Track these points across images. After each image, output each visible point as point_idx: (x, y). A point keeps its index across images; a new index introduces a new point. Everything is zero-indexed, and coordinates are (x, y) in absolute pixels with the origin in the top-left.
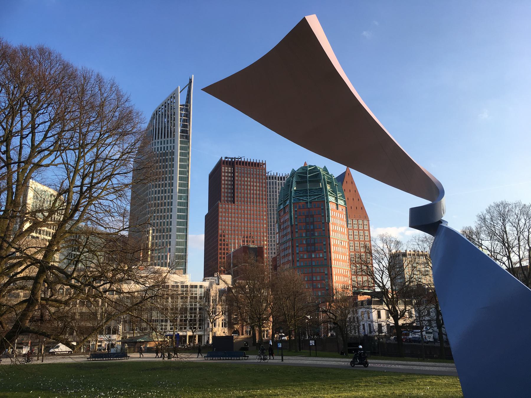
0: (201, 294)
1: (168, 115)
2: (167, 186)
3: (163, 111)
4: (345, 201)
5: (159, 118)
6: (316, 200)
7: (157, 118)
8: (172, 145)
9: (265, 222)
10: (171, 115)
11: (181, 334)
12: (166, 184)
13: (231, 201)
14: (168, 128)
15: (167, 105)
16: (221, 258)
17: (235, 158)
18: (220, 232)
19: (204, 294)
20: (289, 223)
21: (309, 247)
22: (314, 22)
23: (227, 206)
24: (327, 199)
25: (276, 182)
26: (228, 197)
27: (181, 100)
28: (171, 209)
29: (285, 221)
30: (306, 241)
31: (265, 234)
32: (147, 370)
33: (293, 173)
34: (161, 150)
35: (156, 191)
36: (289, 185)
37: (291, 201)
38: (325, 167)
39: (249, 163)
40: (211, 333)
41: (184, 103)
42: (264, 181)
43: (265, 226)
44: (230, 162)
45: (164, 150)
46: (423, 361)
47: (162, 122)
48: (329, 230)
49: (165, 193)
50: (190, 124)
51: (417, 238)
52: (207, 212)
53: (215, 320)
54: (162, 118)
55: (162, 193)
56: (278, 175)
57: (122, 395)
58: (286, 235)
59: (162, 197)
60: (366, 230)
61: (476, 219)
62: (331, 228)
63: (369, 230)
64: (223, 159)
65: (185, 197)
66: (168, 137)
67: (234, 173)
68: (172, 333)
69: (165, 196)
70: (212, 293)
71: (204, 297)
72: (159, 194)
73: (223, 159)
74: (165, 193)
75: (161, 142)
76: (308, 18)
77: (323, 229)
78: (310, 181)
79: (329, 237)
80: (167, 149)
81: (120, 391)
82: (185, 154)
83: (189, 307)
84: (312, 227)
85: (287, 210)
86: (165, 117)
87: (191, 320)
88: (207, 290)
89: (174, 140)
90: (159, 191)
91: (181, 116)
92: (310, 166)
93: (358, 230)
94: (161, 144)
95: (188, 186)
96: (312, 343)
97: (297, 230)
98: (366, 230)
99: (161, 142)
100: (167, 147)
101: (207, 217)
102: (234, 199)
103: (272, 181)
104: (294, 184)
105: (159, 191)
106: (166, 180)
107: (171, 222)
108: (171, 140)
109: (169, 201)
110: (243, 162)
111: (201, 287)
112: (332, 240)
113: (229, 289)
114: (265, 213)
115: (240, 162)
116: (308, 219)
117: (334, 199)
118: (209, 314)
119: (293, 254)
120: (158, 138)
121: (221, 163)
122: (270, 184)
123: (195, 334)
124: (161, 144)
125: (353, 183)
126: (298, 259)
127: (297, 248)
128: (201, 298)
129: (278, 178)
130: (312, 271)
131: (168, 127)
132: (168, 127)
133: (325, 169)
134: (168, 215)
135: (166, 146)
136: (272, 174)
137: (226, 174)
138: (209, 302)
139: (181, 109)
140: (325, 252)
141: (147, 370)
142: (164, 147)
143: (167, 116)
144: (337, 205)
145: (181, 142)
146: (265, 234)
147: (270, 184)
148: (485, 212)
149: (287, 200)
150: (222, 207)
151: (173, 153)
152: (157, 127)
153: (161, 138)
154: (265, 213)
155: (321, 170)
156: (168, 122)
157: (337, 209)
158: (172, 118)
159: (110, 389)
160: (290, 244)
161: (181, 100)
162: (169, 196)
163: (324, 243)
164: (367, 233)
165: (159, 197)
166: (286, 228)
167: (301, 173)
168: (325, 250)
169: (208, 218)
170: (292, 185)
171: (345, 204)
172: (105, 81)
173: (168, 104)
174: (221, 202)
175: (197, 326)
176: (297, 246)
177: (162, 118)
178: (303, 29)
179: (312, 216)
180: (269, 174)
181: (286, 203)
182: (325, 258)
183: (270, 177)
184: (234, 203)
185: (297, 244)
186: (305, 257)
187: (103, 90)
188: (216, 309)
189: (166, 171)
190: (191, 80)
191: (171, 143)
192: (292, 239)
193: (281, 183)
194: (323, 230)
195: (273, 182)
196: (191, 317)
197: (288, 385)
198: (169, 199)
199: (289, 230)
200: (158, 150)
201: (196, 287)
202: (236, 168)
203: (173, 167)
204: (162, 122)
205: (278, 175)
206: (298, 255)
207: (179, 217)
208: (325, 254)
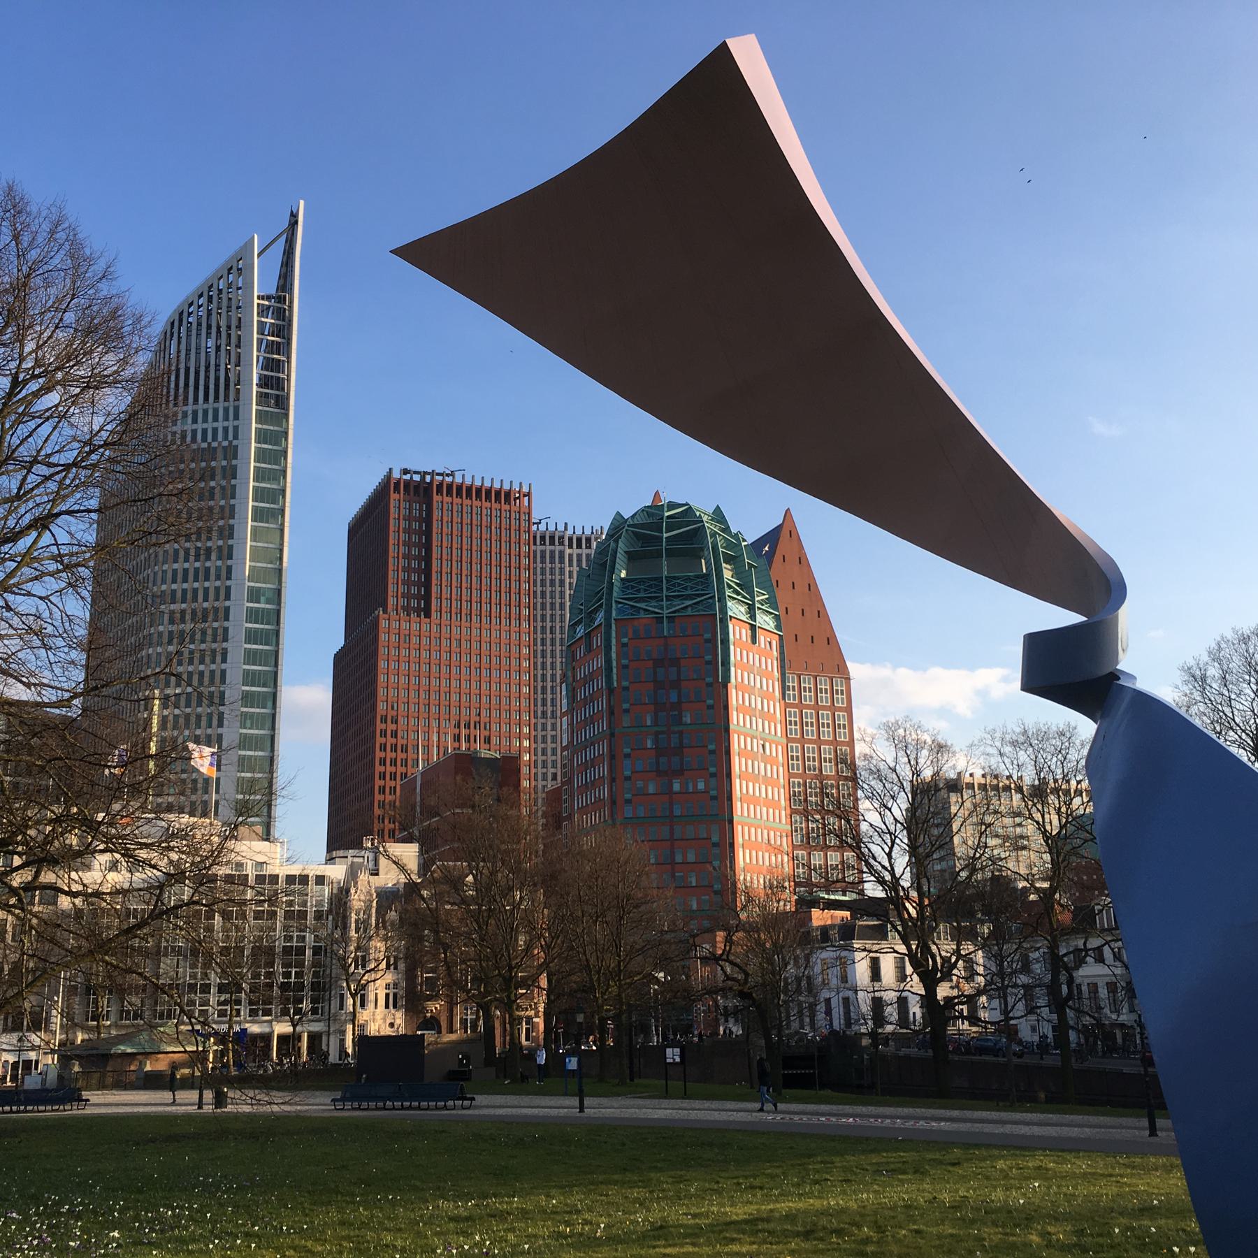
0: (319, 903)
1: (219, 327)
4: (777, 618)
5: (189, 336)
6: (689, 612)
7: (183, 335)
8: (231, 424)
9: (526, 677)
10: (229, 327)
11: (255, 1029)
13: (418, 611)
14: (217, 370)
16: (382, 790)
17: (432, 473)
18: (381, 707)
19: (330, 903)
20: (601, 683)
21: (663, 760)
22: (750, 58)
23: (405, 625)
24: (724, 609)
25: (562, 553)
26: (407, 596)
27: (261, 282)
29: (591, 677)
30: (656, 741)
31: (526, 717)
32: (153, 1141)
33: (619, 525)
36: (603, 562)
37: (608, 613)
38: (718, 511)
39: (479, 490)
40: (350, 1027)
41: (273, 292)
42: (525, 549)
43: (525, 690)
44: (417, 486)
45: (204, 439)
46: (1011, 1108)
47: (198, 348)
48: (726, 707)
49: (207, 579)
50: (289, 358)
51: (998, 735)
52: (339, 642)
53: (364, 987)
54: (198, 335)
55: (196, 579)
56: (570, 532)
57: (78, 1217)
58: (592, 720)
59: (195, 591)
60: (840, 709)
61: (1179, 677)
62: (734, 697)
63: (849, 710)
64: (396, 475)
65: (270, 594)
66: (217, 398)
67: (428, 520)
68: (224, 1028)
69: (206, 590)
70: (357, 900)
71: (330, 911)
72: (185, 580)
73: (396, 475)
75: (195, 413)
76: (735, 45)
77: (710, 702)
78: (670, 553)
79: (727, 730)
80: (215, 438)
81: (71, 1204)
82: (274, 456)
83: (279, 944)
84: (674, 697)
85: (597, 641)
86: (209, 334)
87: (284, 987)
88: (340, 889)
89: (236, 409)
90: (186, 571)
91: (261, 332)
92: (672, 505)
93: (817, 707)
94: (195, 421)
95: (281, 559)
96: (673, 1055)
97: (626, 706)
98: (840, 709)
99: (195, 413)
100: (215, 430)
101: (339, 659)
102: (428, 604)
103: (549, 548)
104: (621, 558)
108: (226, 410)
110: (460, 487)
111: (320, 880)
112: (734, 738)
113: (412, 888)
114: (525, 651)
115: (450, 486)
116: (660, 671)
117: (743, 609)
118: (345, 968)
119: (613, 780)
122: (543, 557)
123: (299, 1029)
124: (195, 421)
125: (802, 560)
126: (628, 796)
127: (627, 762)
128: (319, 916)
129: (570, 539)
130: (672, 833)
131: (217, 366)
132: (217, 366)
133: (718, 515)
135: (210, 425)
136: (552, 528)
138: (345, 927)
139: (263, 311)
140: (713, 775)
141: (153, 1141)
142: (205, 431)
143: (214, 330)
144: (753, 628)
145: (261, 417)
146: (526, 717)
147: (543, 557)
148: (1205, 658)
149: (597, 610)
150: (392, 625)
151: (232, 452)
152: (182, 366)
153: (196, 400)
154: (525, 651)
155: (705, 518)
156: (218, 348)
157: (754, 641)
158: (232, 335)
159: (37, 1200)
160: (604, 748)
161: (261, 282)
162: (217, 589)
163: (711, 747)
164: (842, 719)
166: (592, 699)
167: (642, 526)
168: (712, 770)
169: (342, 662)
170: (614, 562)
171: (778, 627)
172: (33, 208)
173: (220, 291)
174: (385, 612)
175: (305, 1005)
176: (628, 756)
177: (198, 335)
178: (717, 79)
179: (676, 662)
180: (542, 527)
182: (714, 793)
183: (543, 538)
184: (428, 615)
185: (627, 750)
186: (651, 789)
187: (26, 239)
188: (367, 950)
190: (294, 216)
191: (226, 418)
192: (612, 735)
193: (579, 556)
194: (710, 707)
195: (552, 552)
196: (287, 975)
197: (607, 1182)
199: (602, 704)
201: (304, 879)
202: (435, 504)
203: (233, 497)
204: (198, 348)
205: (570, 532)
206: (627, 784)
207: (251, 657)
208: (713, 781)
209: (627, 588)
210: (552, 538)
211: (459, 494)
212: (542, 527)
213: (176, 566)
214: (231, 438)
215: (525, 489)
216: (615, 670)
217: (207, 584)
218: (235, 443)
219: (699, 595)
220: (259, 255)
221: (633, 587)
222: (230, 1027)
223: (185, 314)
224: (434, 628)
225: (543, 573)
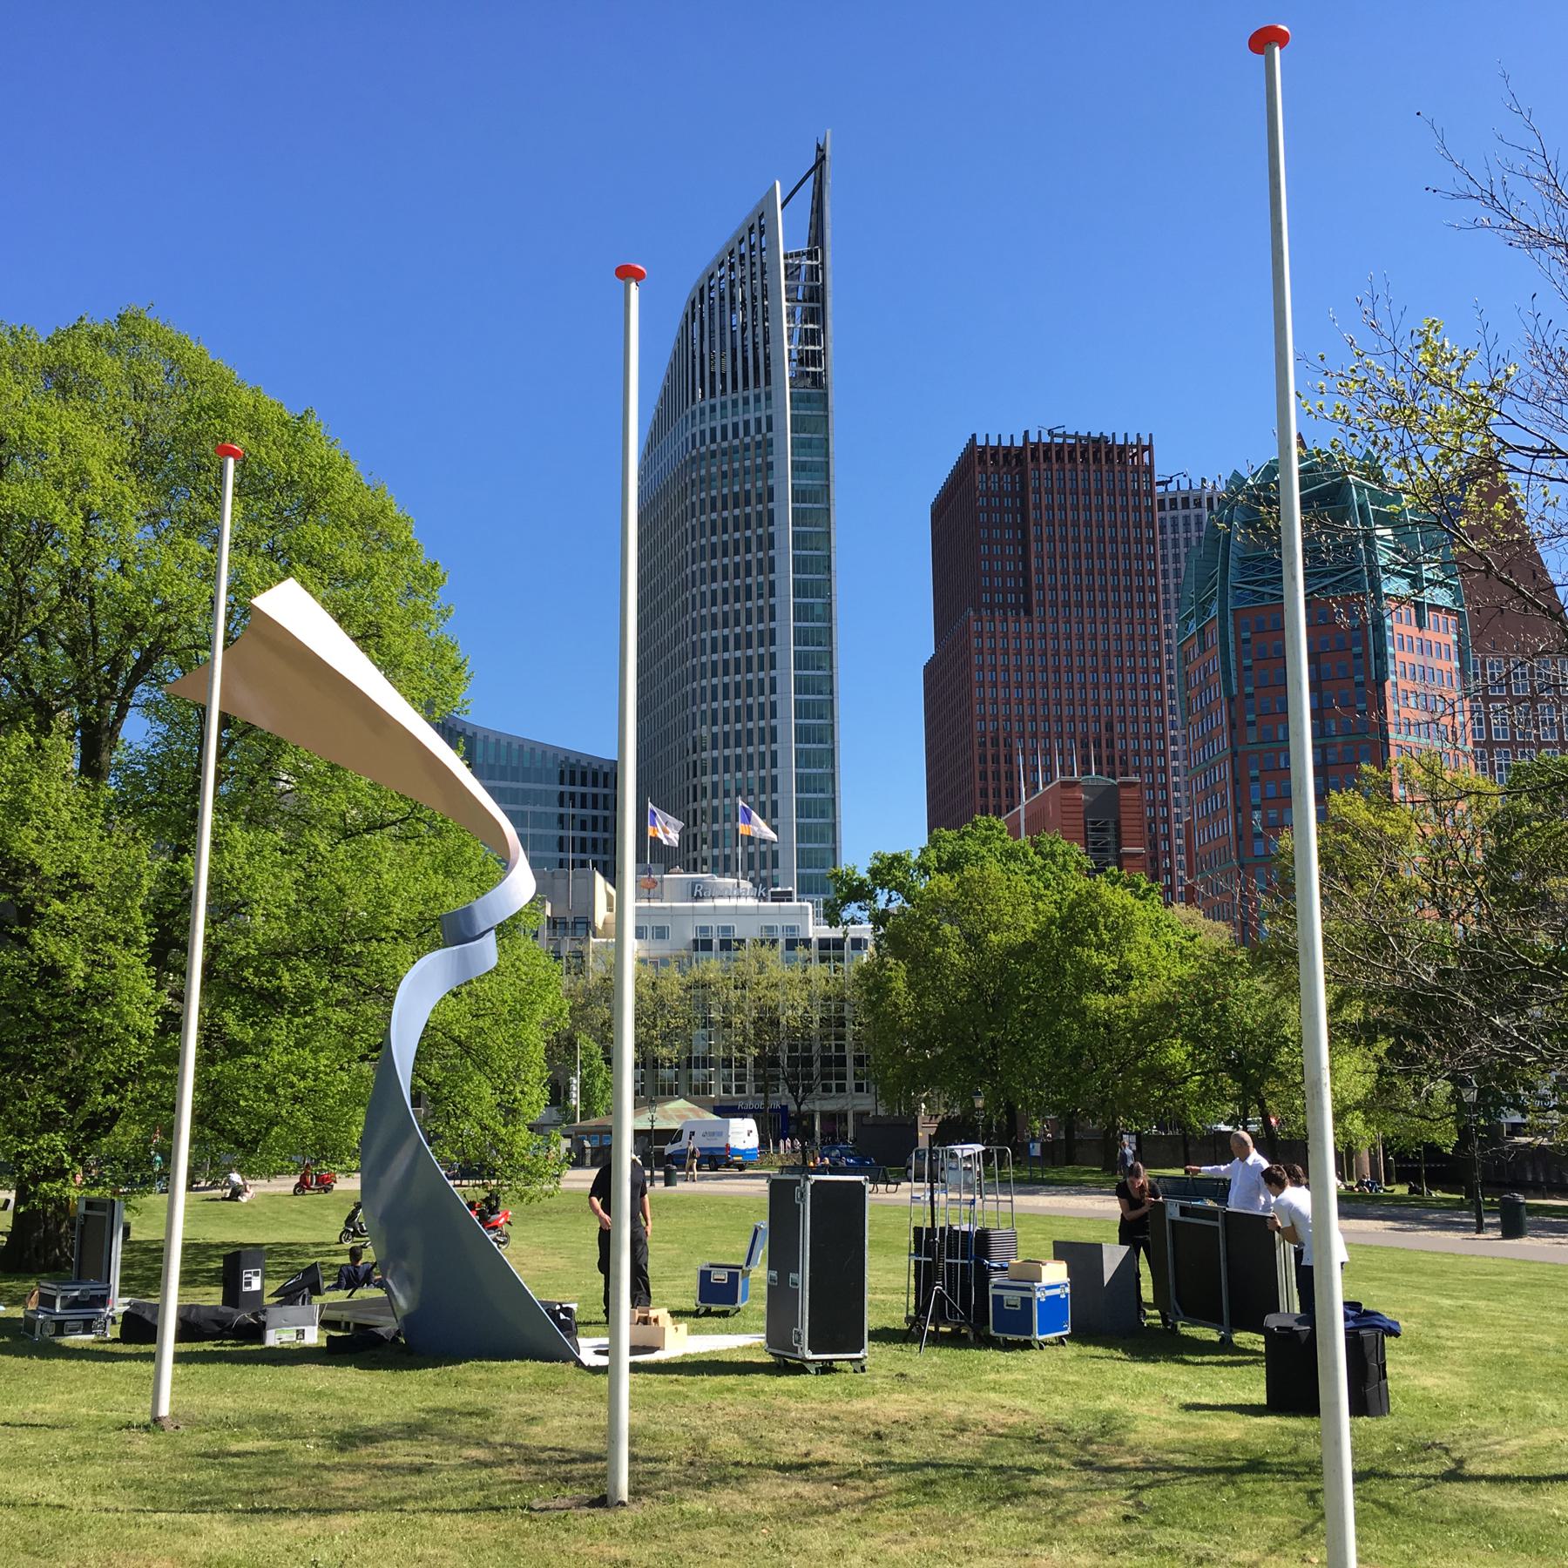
2: (754, 573)
3: (725, 285)
5: (711, 315)
8: (763, 415)
10: (754, 298)
12: (748, 564)
13: (1015, 607)
15: (736, 260)
25: (1199, 518)
27: (786, 237)
34: (724, 438)
35: (714, 592)
45: (736, 435)
47: (722, 328)
49: (749, 598)
52: (930, 651)
54: (722, 312)
59: (737, 612)
66: (746, 384)
69: (749, 611)
74: (749, 598)
80: (747, 433)
86: (733, 310)
90: (725, 591)
97: (1251, 717)
101: (931, 671)
103: (1181, 513)
105: (725, 591)
106: (748, 550)
109: (761, 626)
120: (713, 394)
121: (976, 458)
127: (1255, 786)
129: (1210, 500)
134: (761, 681)
136: (1185, 486)
137: (995, 502)
144: (1419, 606)
149: (1210, 600)
153: (724, 390)
161: (786, 237)
162: (761, 609)
165: (725, 614)
177: (722, 312)
181: (1206, 612)
184: (1028, 612)
185: (1255, 773)
189: (748, 516)
192: (1234, 754)
195: (1186, 518)
198: (761, 620)
200: (713, 440)
204: (722, 328)
209: (1247, 568)
210: (1186, 501)
211: (1059, 458)
212: (1172, 487)
213: (714, 586)
214: (764, 430)
215: (1146, 442)
216: (1234, 674)
217: (749, 604)
218: (769, 435)
219: (1341, 571)
220: (783, 206)
221: (1255, 567)
222: (766, 1104)
223: (706, 290)
225: (1176, 545)
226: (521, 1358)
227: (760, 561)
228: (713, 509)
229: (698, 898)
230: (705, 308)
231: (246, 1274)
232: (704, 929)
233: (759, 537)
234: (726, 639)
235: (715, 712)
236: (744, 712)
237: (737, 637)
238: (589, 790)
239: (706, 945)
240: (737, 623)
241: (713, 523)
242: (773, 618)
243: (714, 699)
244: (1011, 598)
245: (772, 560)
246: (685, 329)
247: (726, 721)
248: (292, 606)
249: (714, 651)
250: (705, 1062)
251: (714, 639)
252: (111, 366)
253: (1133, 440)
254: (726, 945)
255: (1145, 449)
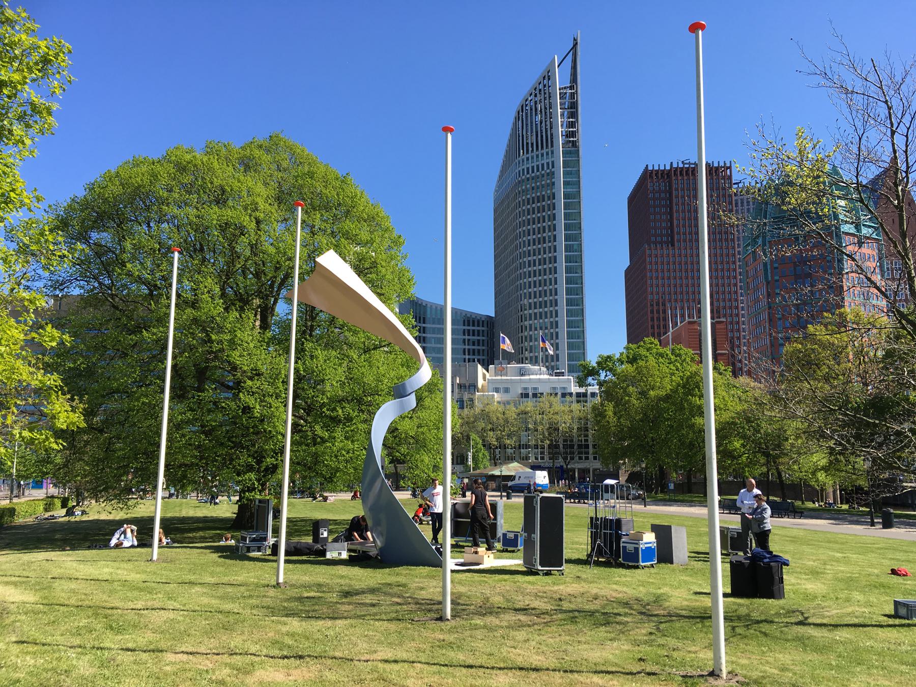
3: (533, 103)
8: (550, 161)
10: (546, 108)
12: (544, 227)
13: (667, 243)
15: (537, 92)
27: (560, 80)
28: (555, 268)
34: (533, 172)
35: (529, 240)
45: (538, 170)
47: (531, 123)
49: (544, 242)
52: (627, 263)
55: (539, 243)
59: (539, 249)
69: (545, 248)
74: (544, 242)
80: (543, 169)
86: (536, 114)
101: (627, 272)
105: (534, 240)
106: (544, 221)
107: (556, 289)
120: (527, 152)
122: (742, 203)
127: (779, 323)
134: (550, 279)
137: (657, 195)
139: (562, 96)
147: (742, 203)
151: (552, 174)
153: (532, 150)
161: (560, 80)
162: (550, 247)
173: (540, 90)
181: (756, 243)
184: (673, 245)
189: (544, 206)
200: (528, 173)
204: (531, 123)
211: (687, 174)
215: (728, 165)
224: (677, 252)
226: (424, 565)
227: (549, 226)
228: (528, 204)
229: (522, 375)
230: (524, 114)
231: (321, 530)
232: (526, 389)
233: (549, 216)
234: (534, 261)
235: (530, 293)
236: (543, 293)
237: (540, 260)
238: (476, 328)
239: (527, 396)
240: (539, 254)
241: (528, 210)
242: (555, 251)
243: (530, 287)
244: (665, 239)
245: (555, 225)
246: (515, 124)
247: (535, 297)
248: (330, 261)
249: (529, 266)
250: (527, 446)
251: (529, 261)
252: (266, 158)
253: (722, 164)
254: (535, 395)
255: (728, 168)
